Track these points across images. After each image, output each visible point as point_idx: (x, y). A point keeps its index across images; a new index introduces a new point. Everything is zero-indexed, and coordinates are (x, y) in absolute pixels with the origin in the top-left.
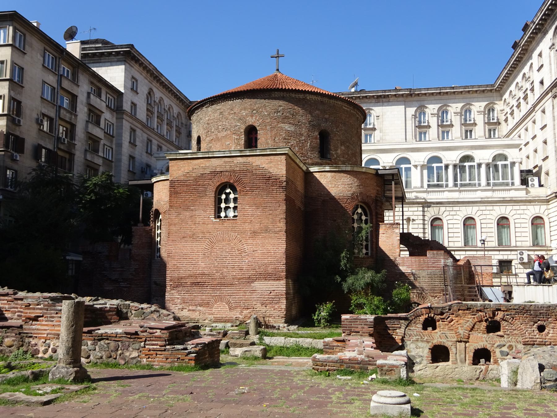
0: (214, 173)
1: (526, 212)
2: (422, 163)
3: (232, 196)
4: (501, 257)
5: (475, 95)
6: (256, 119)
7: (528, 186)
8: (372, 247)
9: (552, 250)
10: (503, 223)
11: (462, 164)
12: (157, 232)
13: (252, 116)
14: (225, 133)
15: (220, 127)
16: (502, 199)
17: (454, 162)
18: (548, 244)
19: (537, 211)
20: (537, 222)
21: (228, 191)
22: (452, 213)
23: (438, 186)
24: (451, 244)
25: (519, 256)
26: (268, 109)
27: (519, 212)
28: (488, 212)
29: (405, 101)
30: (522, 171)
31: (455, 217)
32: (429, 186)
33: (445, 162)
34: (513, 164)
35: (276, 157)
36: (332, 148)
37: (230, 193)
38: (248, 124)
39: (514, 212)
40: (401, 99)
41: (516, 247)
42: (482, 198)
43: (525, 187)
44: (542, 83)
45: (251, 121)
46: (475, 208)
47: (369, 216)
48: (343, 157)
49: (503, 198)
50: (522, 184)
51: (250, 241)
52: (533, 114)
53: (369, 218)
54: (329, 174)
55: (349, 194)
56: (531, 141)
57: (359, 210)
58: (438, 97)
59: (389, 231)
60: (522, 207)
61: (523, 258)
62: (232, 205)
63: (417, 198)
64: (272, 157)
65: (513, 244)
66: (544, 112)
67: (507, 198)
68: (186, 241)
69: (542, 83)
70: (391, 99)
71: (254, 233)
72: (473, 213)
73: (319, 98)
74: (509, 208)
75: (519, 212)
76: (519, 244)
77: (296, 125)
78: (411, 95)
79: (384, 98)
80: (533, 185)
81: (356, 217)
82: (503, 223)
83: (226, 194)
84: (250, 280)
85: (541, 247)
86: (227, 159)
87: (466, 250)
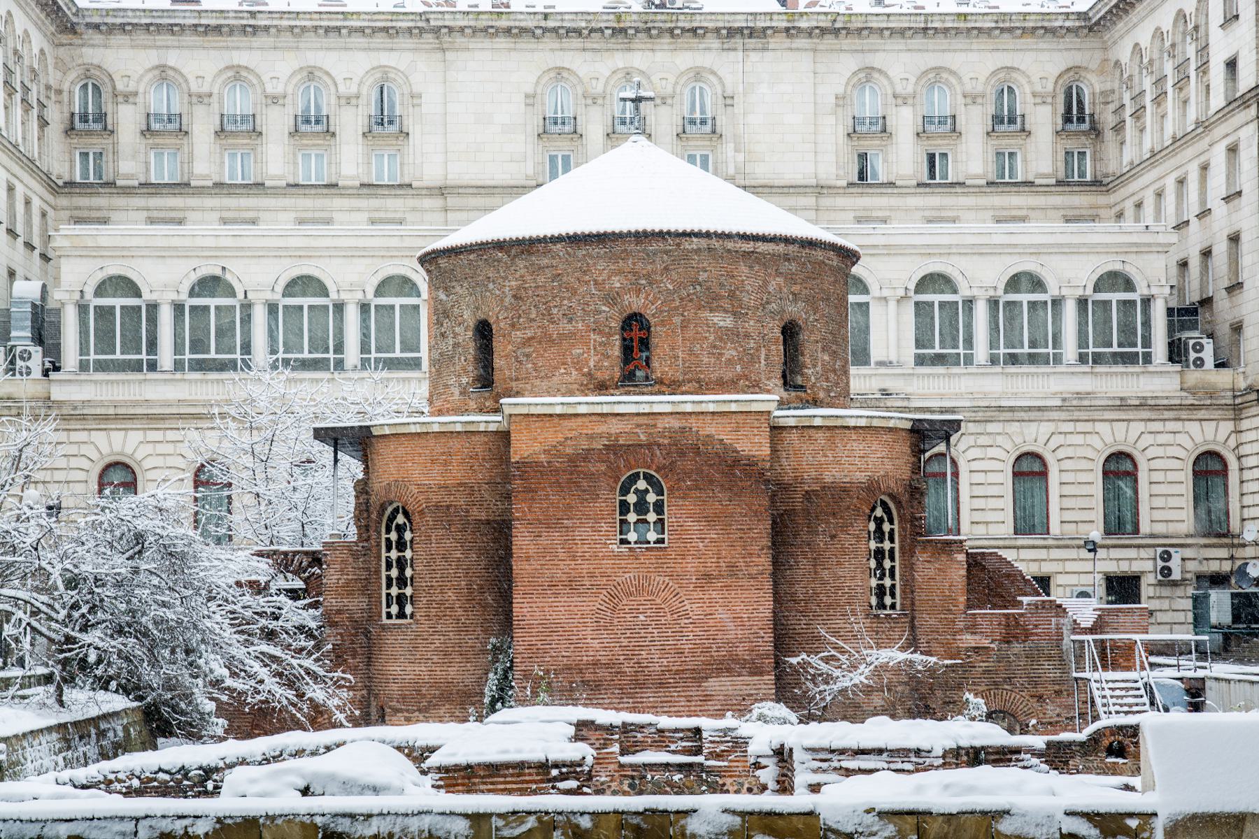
0: (613, 448)
1: (1181, 439)
2: (901, 293)
3: (651, 498)
4: (1112, 568)
5: (1028, 41)
6: (646, 298)
7: (1188, 366)
8: (903, 592)
9: (1244, 546)
10: (1119, 469)
11: (1012, 297)
12: (384, 554)
13: (638, 292)
14: (569, 327)
15: (555, 311)
16: (1118, 403)
17: (991, 293)
18: (1235, 524)
19: (1210, 437)
20: (1209, 470)
21: (642, 484)
22: (983, 440)
23: (939, 360)
24: (980, 530)
25: (1160, 564)
26: (675, 276)
27: (1162, 439)
28: (1079, 439)
29: (815, 50)
30: (1170, 311)
31: (991, 452)
32: (920, 361)
33: (965, 292)
34: (1147, 301)
35: (750, 419)
36: (808, 361)
37: (647, 491)
38: (629, 312)
39: (1147, 440)
40: (802, 42)
41: (1152, 536)
42: (1064, 400)
43: (1178, 367)
44: (1232, 65)
45: (635, 303)
46: (1046, 428)
47: (896, 522)
48: (827, 380)
49: (1122, 399)
50: (1171, 359)
51: (696, 595)
52: (1203, 144)
53: (896, 527)
54: (820, 434)
55: (861, 477)
56: (1194, 221)
57: (879, 512)
58: (918, 42)
59: (944, 558)
60: (1171, 426)
61: (1169, 569)
62: (652, 517)
63: (886, 393)
64: (740, 418)
65: (1145, 527)
66: (1233, 150)
67: (1130, 398)
68: (556, 595)
69: (1232, 65)
70: (774, 42)
71: (707, 578)
72: (1042, 440)
73: (781, 248)
74: (1140, 427)
75: (1162, 439)
76: (1160, 528)
77: (734, 314)
78: (836, 32)
79: (751, 36)
80: (1199, 363)
81: (872, 526)
82: (1119, 469)
83: (637, 491)
84: (699, 676)
85: (1219, 536)
86: (641, 420)
87: (1018, 548)
